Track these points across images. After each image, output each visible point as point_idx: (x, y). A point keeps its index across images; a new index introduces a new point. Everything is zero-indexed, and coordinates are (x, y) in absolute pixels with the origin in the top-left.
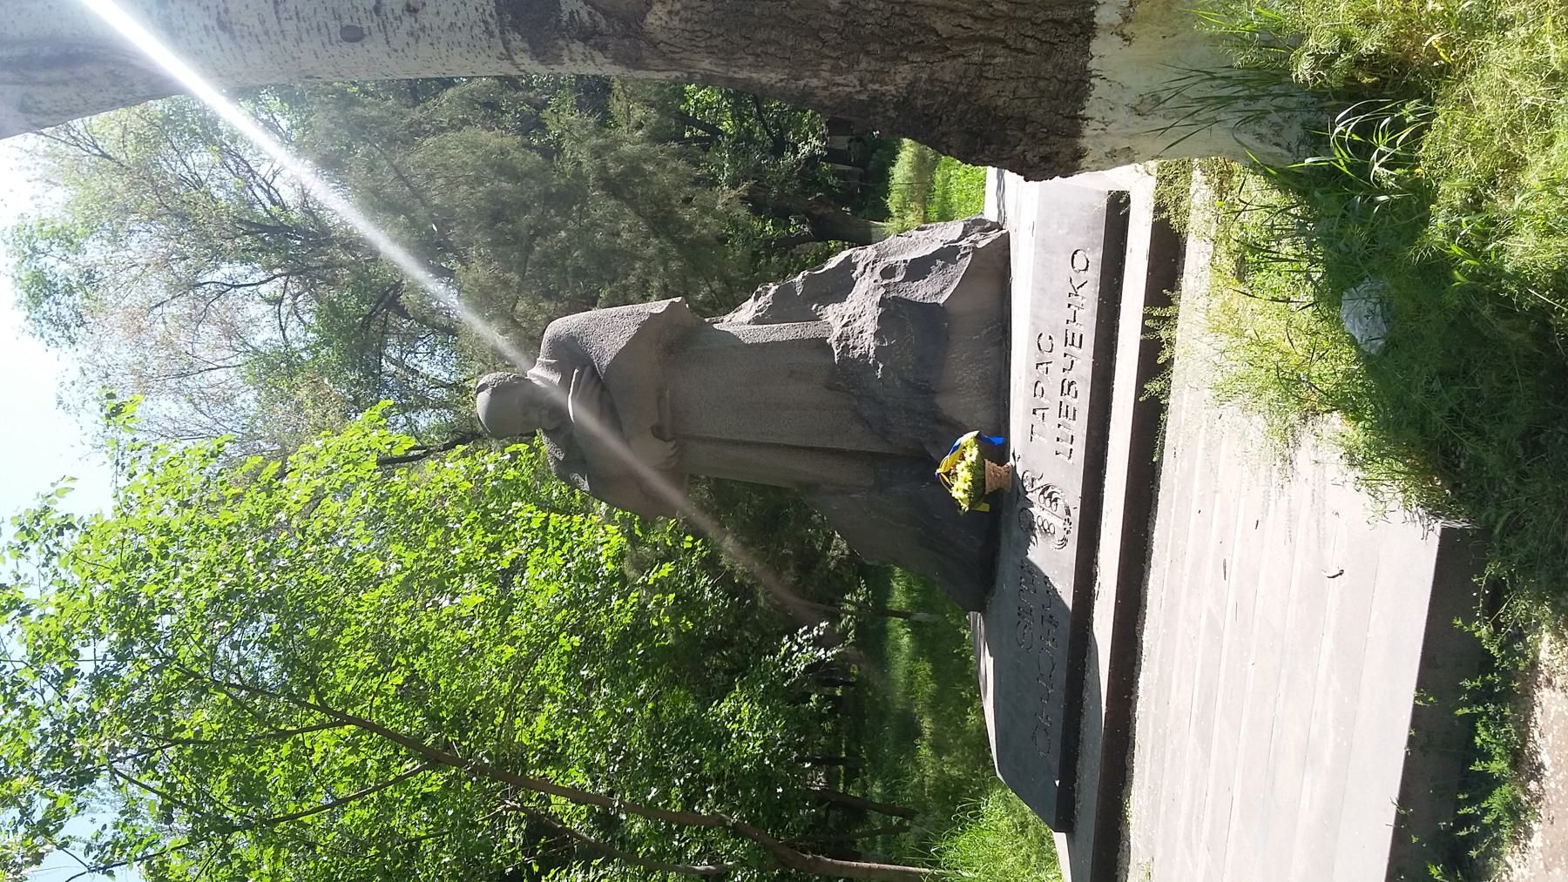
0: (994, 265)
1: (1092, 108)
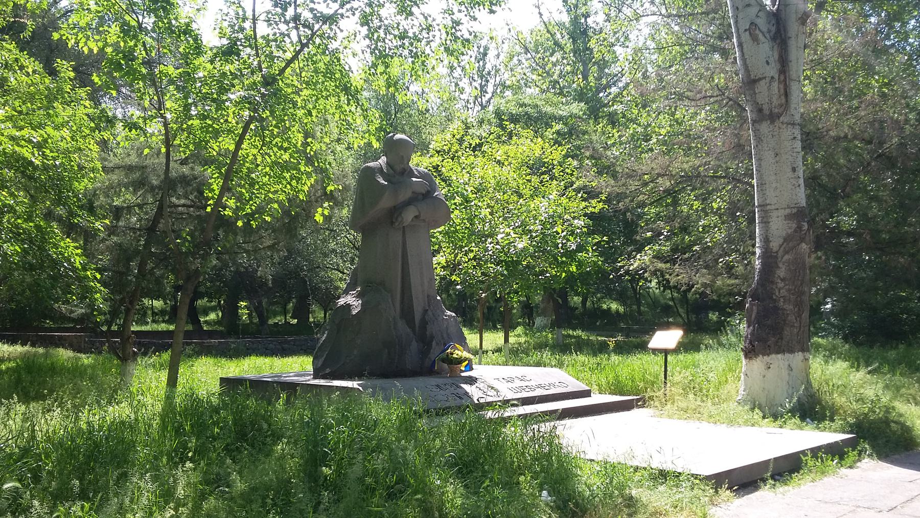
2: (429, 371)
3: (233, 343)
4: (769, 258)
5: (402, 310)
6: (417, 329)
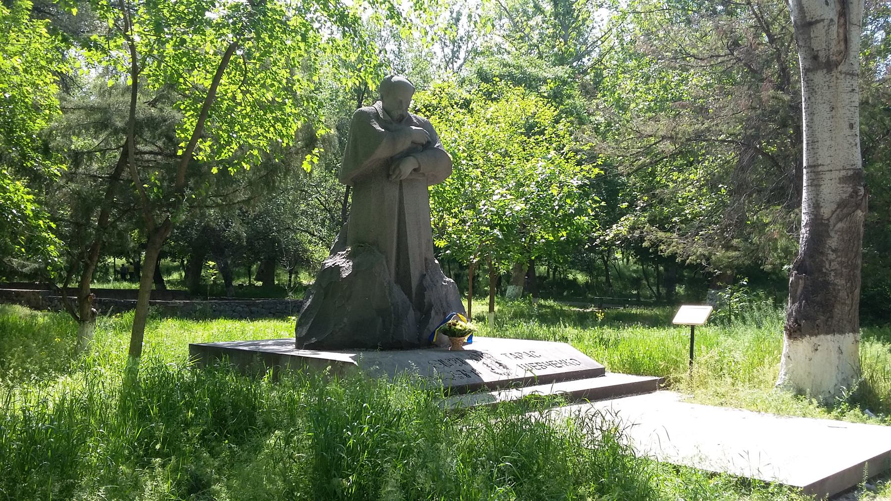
1: (837, 336)
2: (428, 344)
3: (199, 304)
4: (819, 227)
5: (397, 273)
6: (414, 295)
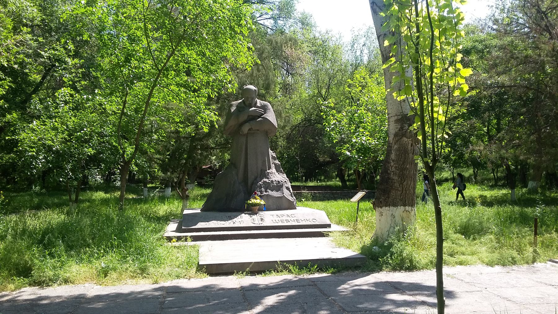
0: (291, 206)
1: (391, 208)
